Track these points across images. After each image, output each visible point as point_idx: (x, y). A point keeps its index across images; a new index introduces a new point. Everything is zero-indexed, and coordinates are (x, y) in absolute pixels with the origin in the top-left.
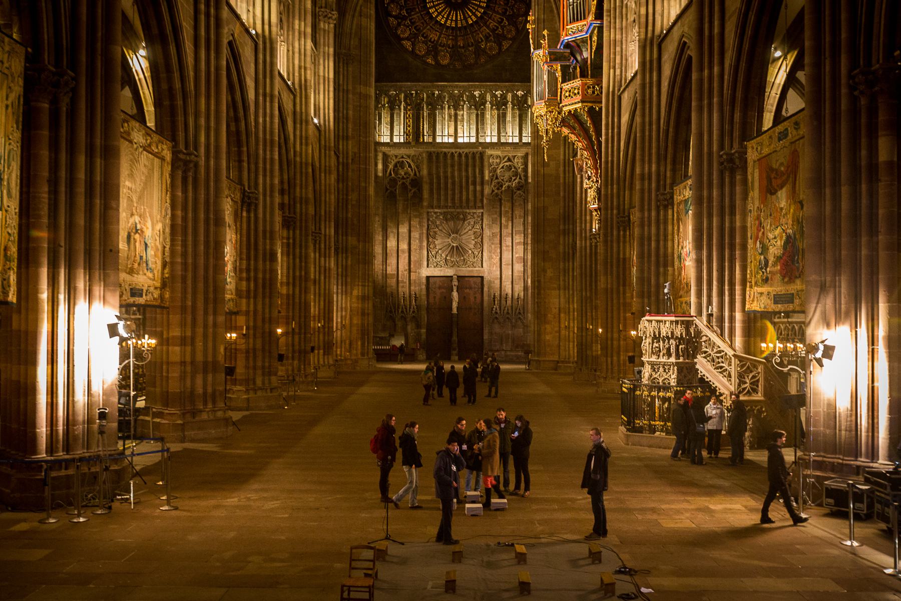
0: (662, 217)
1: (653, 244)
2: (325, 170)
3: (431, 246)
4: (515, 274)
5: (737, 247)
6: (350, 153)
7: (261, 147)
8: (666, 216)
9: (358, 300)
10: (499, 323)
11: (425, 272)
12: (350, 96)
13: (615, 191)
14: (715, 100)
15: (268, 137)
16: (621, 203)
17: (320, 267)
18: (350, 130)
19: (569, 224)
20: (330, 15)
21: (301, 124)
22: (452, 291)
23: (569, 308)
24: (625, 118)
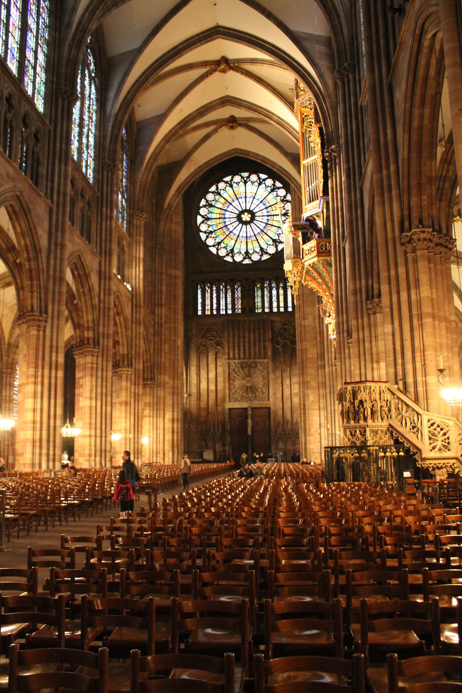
0: (372, 322)
3: (232, 387)
5: (423, 316)
6: (163, 316)
7: (51, 282)
8: (375, 320)
10: (283, 441)
11: (228, 405)
12: (164, 277)
13: (345, 318)
15: (58, 274)
17: (131, 392)
18: (163, 300)
20: (140, 215)
21: (105, 280)
22: (247, 418)
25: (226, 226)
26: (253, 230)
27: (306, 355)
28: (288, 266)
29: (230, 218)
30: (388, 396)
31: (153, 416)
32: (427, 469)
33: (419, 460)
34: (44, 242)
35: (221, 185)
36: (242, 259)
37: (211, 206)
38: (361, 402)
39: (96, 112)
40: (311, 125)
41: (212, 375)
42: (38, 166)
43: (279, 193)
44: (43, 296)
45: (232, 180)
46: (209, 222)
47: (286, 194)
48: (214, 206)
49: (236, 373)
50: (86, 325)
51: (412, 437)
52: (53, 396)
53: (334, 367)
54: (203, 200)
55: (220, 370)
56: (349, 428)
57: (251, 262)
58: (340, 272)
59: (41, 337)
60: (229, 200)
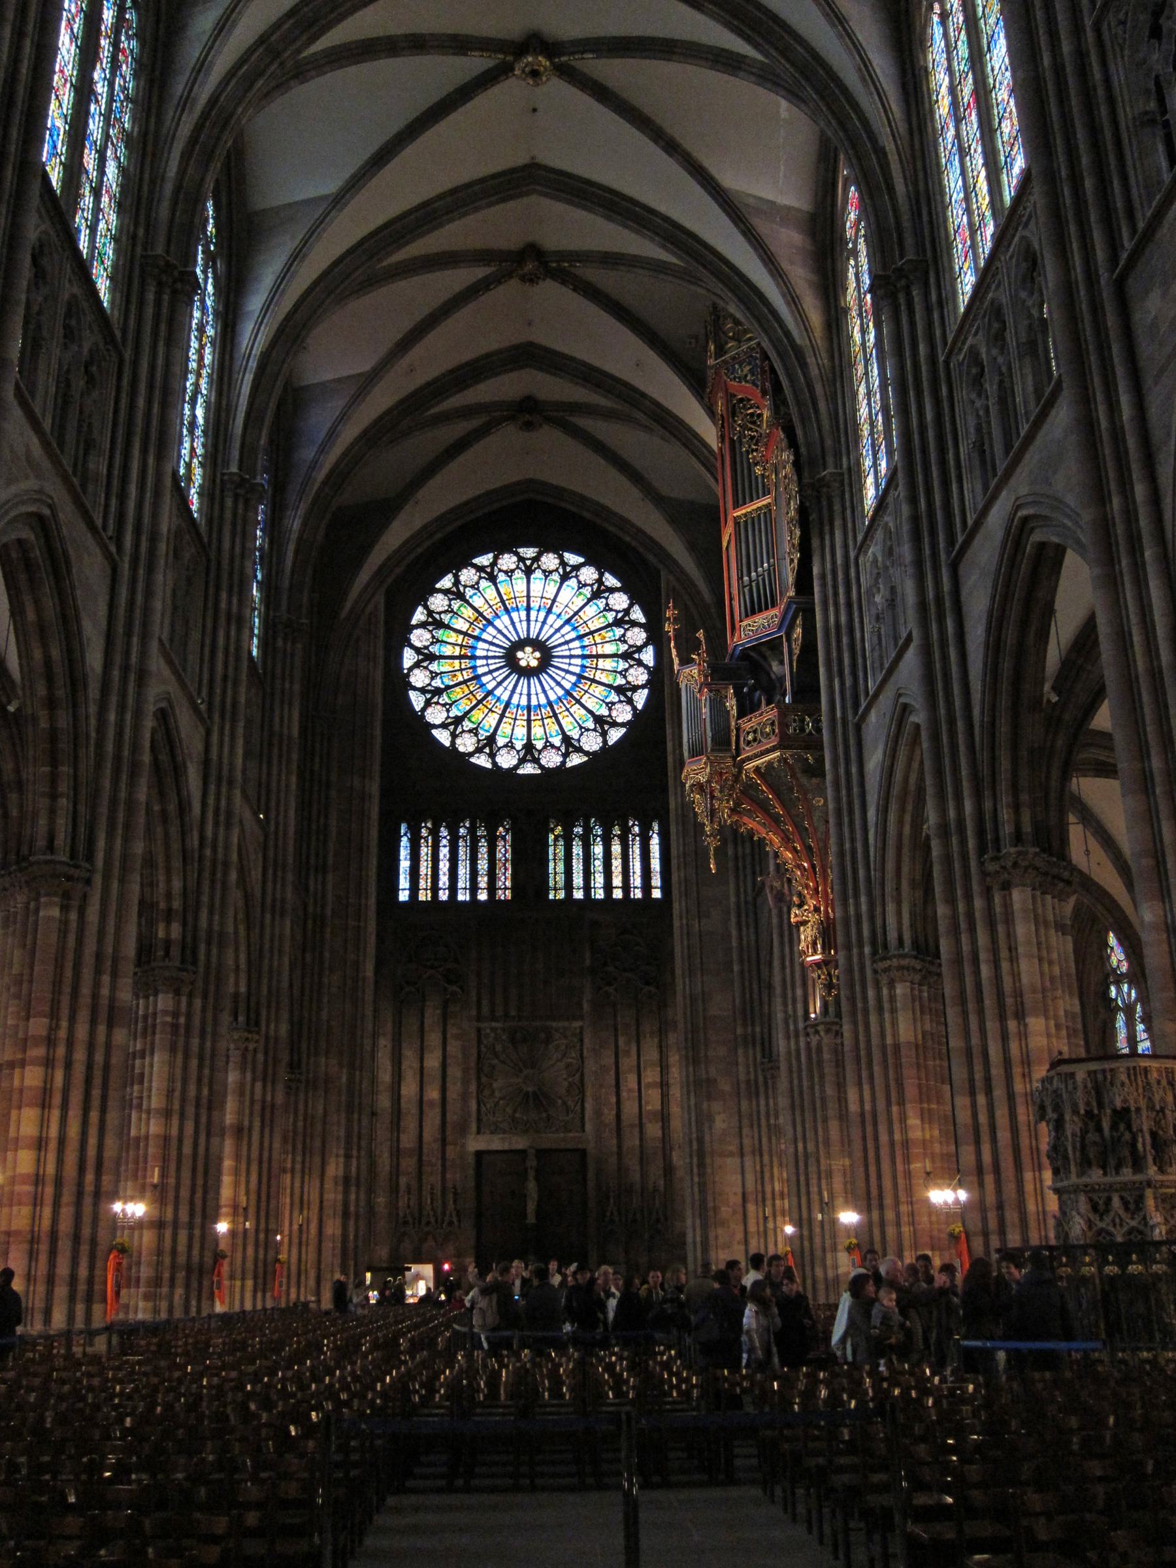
0: (998, 909)
1: (985, 971)
2: (273, 907)
3: (487, 1092)
6: (330, 897)
8: (1007, 905)
9: (336, 1183)
11: (475, 1144)
12: (333, 793)
14: (1148, 554)
16: (879, 930)
17: (252, 1102)
19: (753, 1025)
21: (219, 786)
23: (763, 1192)
24: (874, 760)
25: (477, 677)
26: (544, 691)
27: (705, 1010)
28: (696, 771)
29: (487, 658)
31: (293, 1171)
34: (94, 659)
35: (468, 575)
36: (515, 762)
37: (440, 625)
38: (1122, 1116)
39: (213, 343)
40: (754, 423)
41: (433, 1062)
42: (86, 454)
43: (611, 601)
44: (82, 808)
45: (494, 564)
46: (434, 667)
47: (631, 606)
48: (448, 627)
49: (497, 1057)
50: (162, 905)
52: (96, 1103)
54: (420, 609)
55: (454, 1048)
56: (1088, 1189)
58: (849, 789)
59: (73, 926)
60: (488, 614)
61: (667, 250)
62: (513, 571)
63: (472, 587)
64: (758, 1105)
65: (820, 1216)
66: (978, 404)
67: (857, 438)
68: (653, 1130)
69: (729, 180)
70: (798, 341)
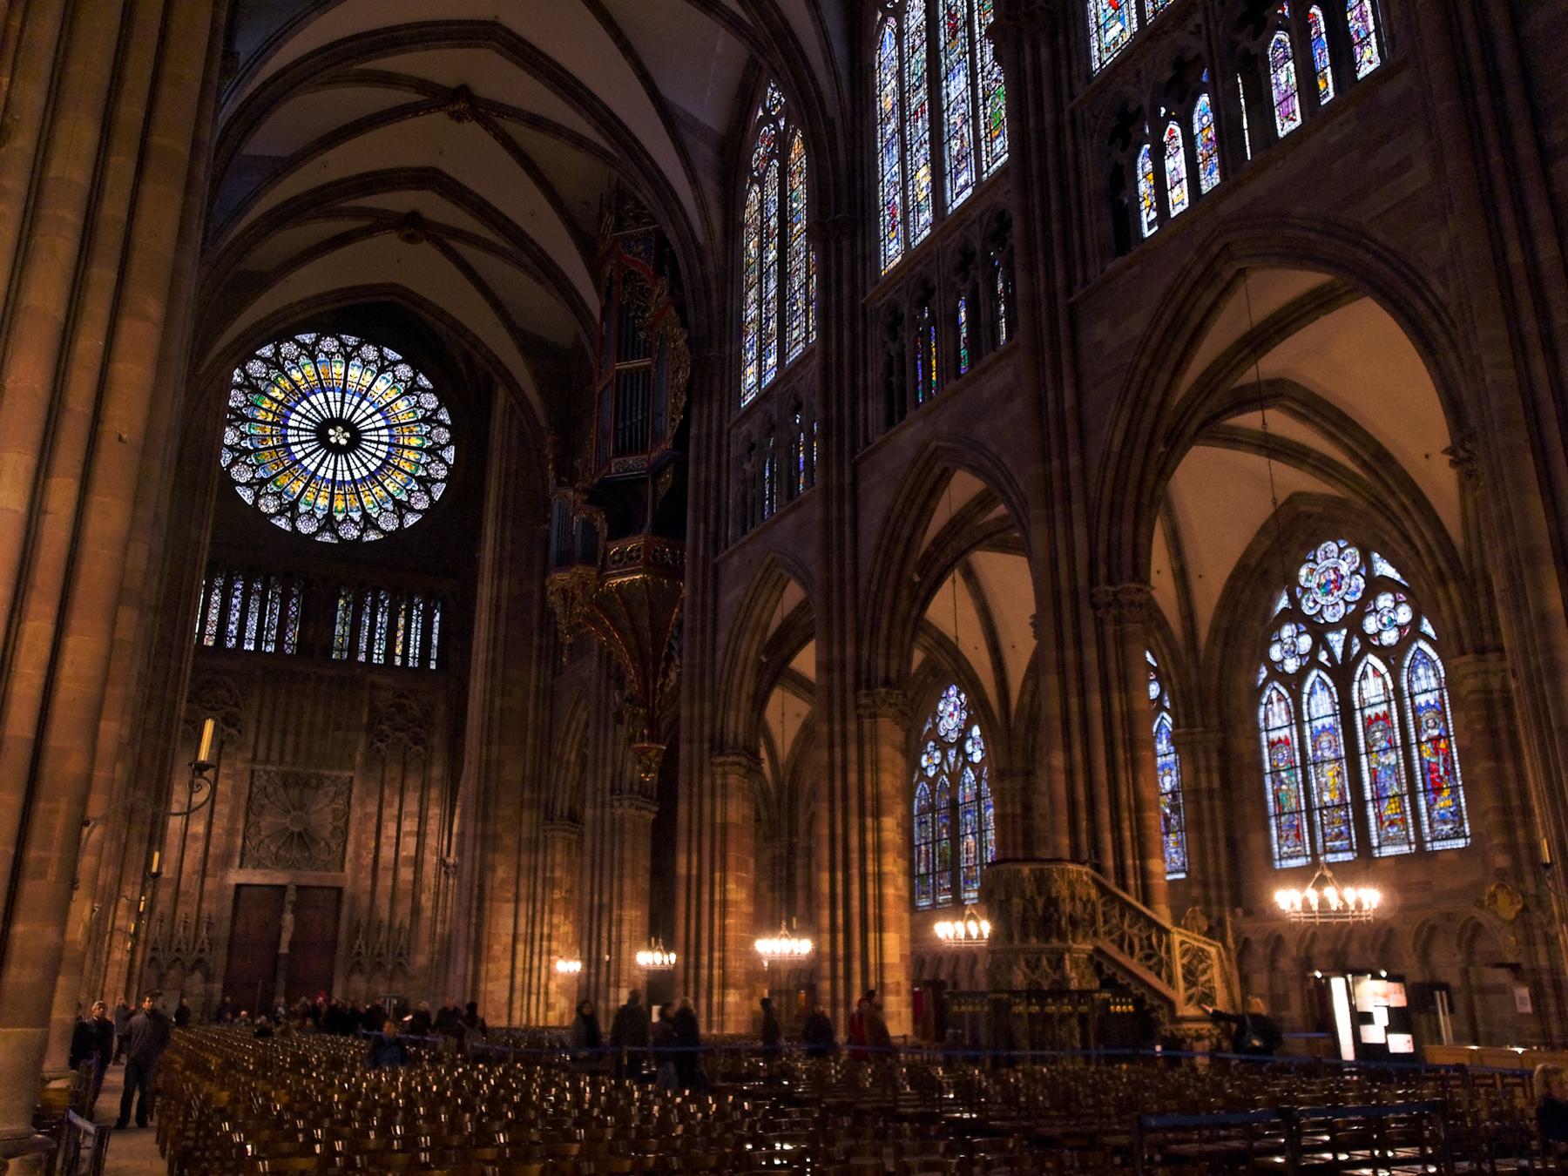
3: (252, 830)
4: (401, 885)
11: (235, 877)
25: (287, 446)
29: (298, 429)
30: (1094, 893)
32: (1183, 1040)
33: (1166, 1020)
35: (288, 349)
36: (313, 529)
37: (255, 389)
40: (643, 295)
45: (316, 343)
46: (245, 428)
49: (267, 797)
51: (1151, 979)
53: (608, 810)
57: (336, 542)
60: (303, 386)
61: (598, 130)
62: (333, 354)
63: (292, 361)
64: (536, 862)
65: (607, 957)
66: (890, 345)
67: (741, 332)
68: (406, 874)
69: (666, 89)
70: (701, 239)
